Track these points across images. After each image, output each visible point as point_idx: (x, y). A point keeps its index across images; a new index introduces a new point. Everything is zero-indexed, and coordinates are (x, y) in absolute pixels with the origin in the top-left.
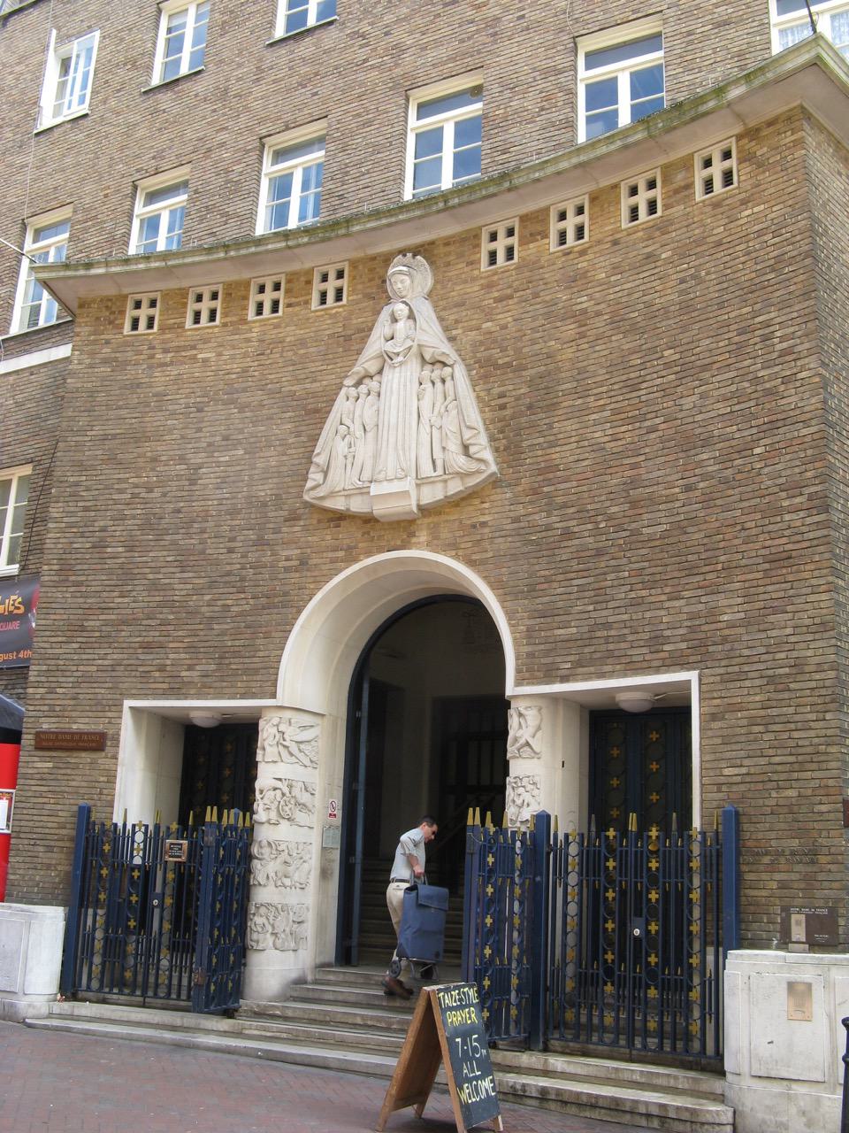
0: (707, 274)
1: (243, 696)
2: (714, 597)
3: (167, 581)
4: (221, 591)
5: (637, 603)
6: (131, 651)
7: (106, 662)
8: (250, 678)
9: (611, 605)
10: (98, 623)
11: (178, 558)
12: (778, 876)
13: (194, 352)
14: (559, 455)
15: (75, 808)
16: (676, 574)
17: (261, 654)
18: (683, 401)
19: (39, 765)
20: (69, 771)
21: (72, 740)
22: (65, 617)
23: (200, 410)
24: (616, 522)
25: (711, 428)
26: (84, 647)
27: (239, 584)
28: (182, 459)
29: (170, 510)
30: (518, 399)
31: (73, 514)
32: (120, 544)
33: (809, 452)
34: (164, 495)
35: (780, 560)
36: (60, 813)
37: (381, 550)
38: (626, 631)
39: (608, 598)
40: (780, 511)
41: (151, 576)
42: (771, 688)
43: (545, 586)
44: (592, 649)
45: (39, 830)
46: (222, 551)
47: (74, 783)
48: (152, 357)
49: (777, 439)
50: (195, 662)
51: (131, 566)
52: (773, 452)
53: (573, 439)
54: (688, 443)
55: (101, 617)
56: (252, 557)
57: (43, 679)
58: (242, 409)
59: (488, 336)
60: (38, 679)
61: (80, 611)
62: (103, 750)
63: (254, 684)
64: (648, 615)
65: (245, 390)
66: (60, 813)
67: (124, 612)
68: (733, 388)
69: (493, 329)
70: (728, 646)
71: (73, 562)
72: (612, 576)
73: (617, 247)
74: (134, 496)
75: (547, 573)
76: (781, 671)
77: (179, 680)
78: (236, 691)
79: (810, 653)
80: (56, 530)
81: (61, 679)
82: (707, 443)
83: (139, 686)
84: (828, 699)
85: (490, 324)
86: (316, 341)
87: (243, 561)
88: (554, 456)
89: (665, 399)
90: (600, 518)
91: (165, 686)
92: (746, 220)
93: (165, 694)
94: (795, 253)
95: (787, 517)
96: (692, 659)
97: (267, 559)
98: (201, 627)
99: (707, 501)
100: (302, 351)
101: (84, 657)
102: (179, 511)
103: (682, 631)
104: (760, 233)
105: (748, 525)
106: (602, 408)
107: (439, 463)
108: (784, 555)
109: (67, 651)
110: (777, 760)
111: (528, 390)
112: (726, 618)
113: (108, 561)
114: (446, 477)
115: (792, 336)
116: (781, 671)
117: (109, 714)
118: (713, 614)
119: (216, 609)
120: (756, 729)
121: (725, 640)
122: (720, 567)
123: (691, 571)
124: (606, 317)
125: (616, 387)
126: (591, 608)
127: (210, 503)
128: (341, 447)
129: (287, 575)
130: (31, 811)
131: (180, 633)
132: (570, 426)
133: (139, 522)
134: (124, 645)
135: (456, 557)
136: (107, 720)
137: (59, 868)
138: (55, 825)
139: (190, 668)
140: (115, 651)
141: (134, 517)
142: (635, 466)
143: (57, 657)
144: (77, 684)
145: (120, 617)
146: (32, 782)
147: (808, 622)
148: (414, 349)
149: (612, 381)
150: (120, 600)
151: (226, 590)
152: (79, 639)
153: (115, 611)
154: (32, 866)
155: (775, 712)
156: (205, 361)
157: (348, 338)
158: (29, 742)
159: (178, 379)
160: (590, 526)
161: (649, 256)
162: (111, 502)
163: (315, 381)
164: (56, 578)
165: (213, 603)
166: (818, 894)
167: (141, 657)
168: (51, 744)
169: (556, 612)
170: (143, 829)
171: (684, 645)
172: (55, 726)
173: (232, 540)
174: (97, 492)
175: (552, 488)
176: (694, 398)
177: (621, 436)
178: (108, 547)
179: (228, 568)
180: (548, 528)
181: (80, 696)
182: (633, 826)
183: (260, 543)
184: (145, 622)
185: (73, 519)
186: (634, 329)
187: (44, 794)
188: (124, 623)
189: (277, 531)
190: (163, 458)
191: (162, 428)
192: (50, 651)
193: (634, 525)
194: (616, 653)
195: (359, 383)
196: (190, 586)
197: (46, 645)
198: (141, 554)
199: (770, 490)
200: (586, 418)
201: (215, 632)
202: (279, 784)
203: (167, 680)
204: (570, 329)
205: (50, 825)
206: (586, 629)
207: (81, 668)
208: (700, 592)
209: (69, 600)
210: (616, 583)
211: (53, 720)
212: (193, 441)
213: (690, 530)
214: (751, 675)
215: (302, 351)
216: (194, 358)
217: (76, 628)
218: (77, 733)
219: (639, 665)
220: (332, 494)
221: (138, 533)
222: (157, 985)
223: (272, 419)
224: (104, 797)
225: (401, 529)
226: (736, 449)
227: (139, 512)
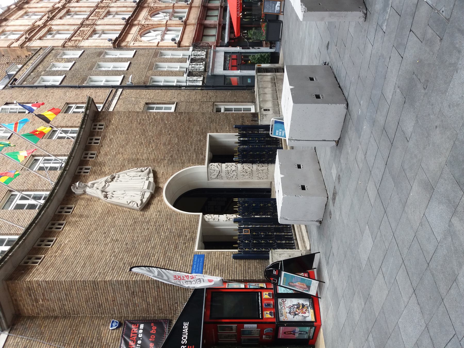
1: (198, 223)
3: (153, 244)
5: (191, 144)
6: (176, 252)
7: (179, 258)
10: (163, 261)
13: (63, 244)
14: (152, 157)
20: (220, 265)
35: (189, 120)
36: (236, 266)
41: (149, 249)
50: (184, 235)
52: (168, 120)
54: (160, 134)
55: (161, 261)
58: (96, 229)
65: (89, 229)
66: (236, 266)
82: (161, 131)
83: (190, 248)
91: (191, 242)
98: (172, 234)
118: (197, 131)
121: (202, 129)
123: (187, 134)
134: (174, 254)
137: (256, 265)
138: (240, 267)
139: (186, 236)
142: (160, 144)
150: (156, 257)
153: (160, 257)
167: (179, 249)
173: (144, 229)
183: (148, 222)
185: (115, 273)
190: (103, 249)
201: (175, 231)
205: (240, 269)
207: (180, 265)
220: (142, 200)
225: (157, 190)
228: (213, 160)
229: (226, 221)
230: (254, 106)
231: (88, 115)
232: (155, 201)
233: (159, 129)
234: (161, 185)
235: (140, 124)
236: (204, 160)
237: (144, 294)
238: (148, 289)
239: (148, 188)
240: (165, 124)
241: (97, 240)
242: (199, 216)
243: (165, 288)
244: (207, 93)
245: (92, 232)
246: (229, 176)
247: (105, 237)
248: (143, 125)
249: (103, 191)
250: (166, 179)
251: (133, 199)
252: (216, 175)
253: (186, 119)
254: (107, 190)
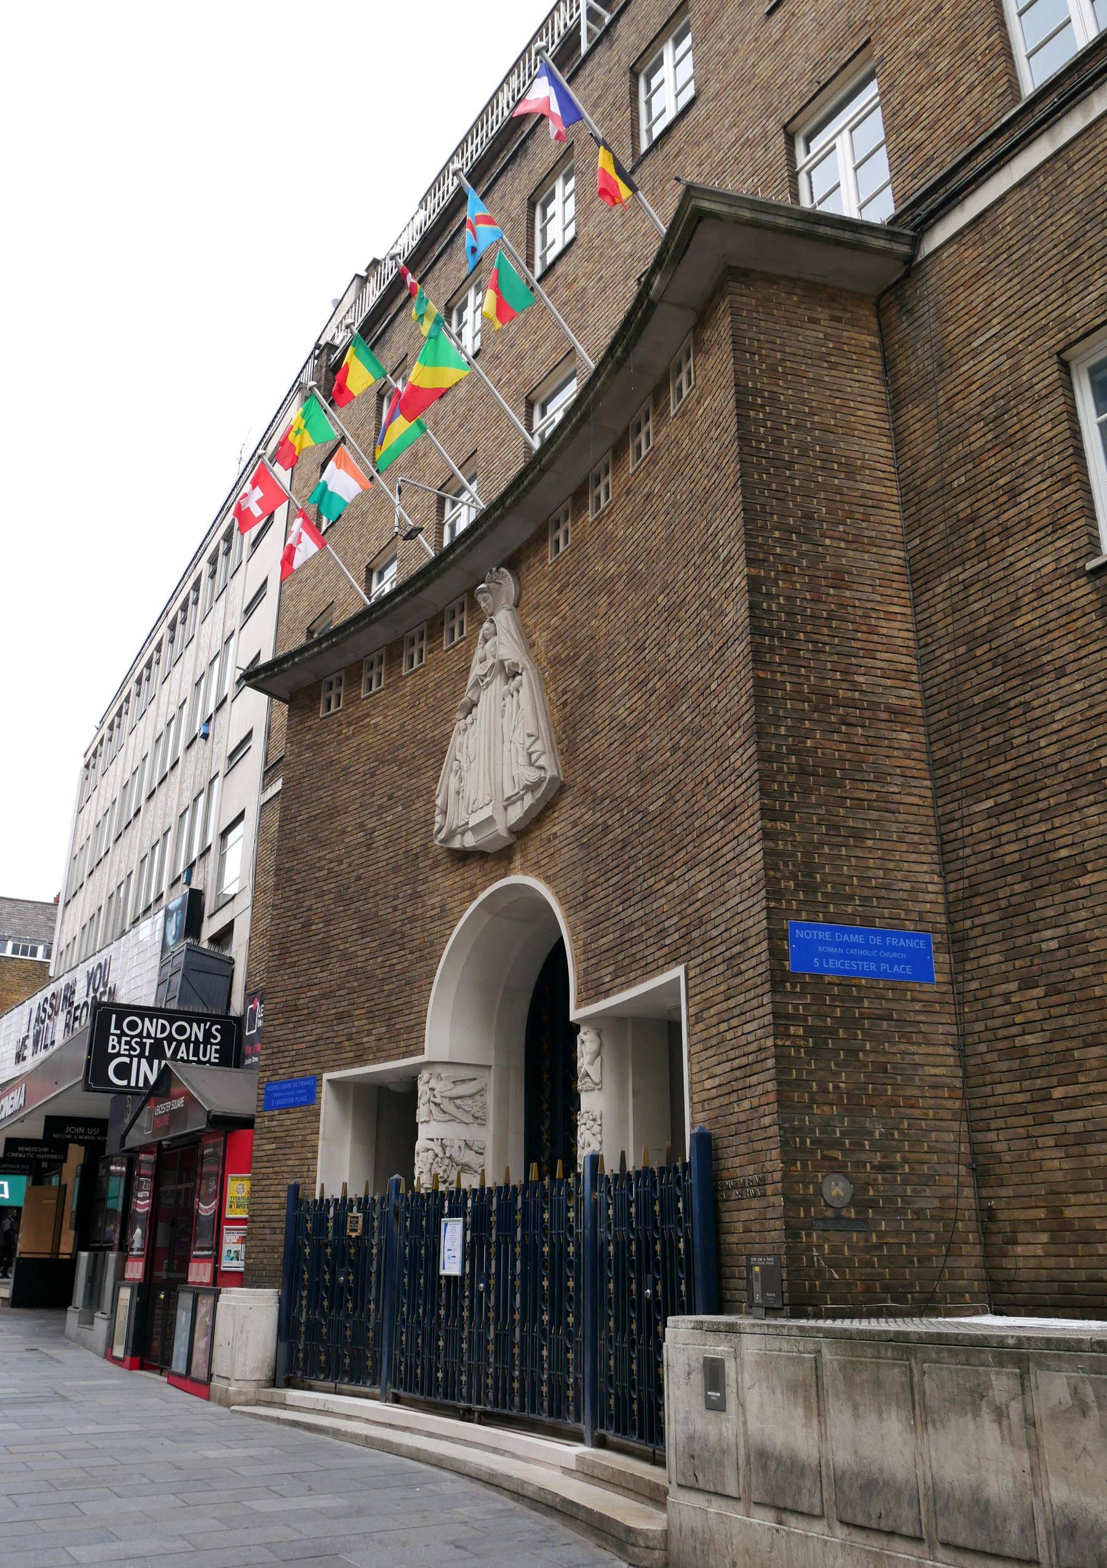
4: (388, 951)
20: (287, 1151)
23: (373, 775)
26: (299, 1024)
47: (290, 1163)
50: (371, 1027)
55: (309, 994)
61: (294, 991)
67: (323, 986)
71: (289, 945)
77: (361, 1047)
83: (335, 1057)
91: (352, 1054)
93: (351, 1064)
98: (375, 990)
128: (453, 782)
138: (277, 1206)
139: (369, 1033)
146: (262, 1165)
148: (497, 666)
152: (294, 1019)
153: (318, 987)
156: (376, 725)
162: (314, 881)
173: (396, 898)
188: (324, 996)
202: (431, 1145)
205: (275, 1206)
227: (333, 885)
234: (518, 861)
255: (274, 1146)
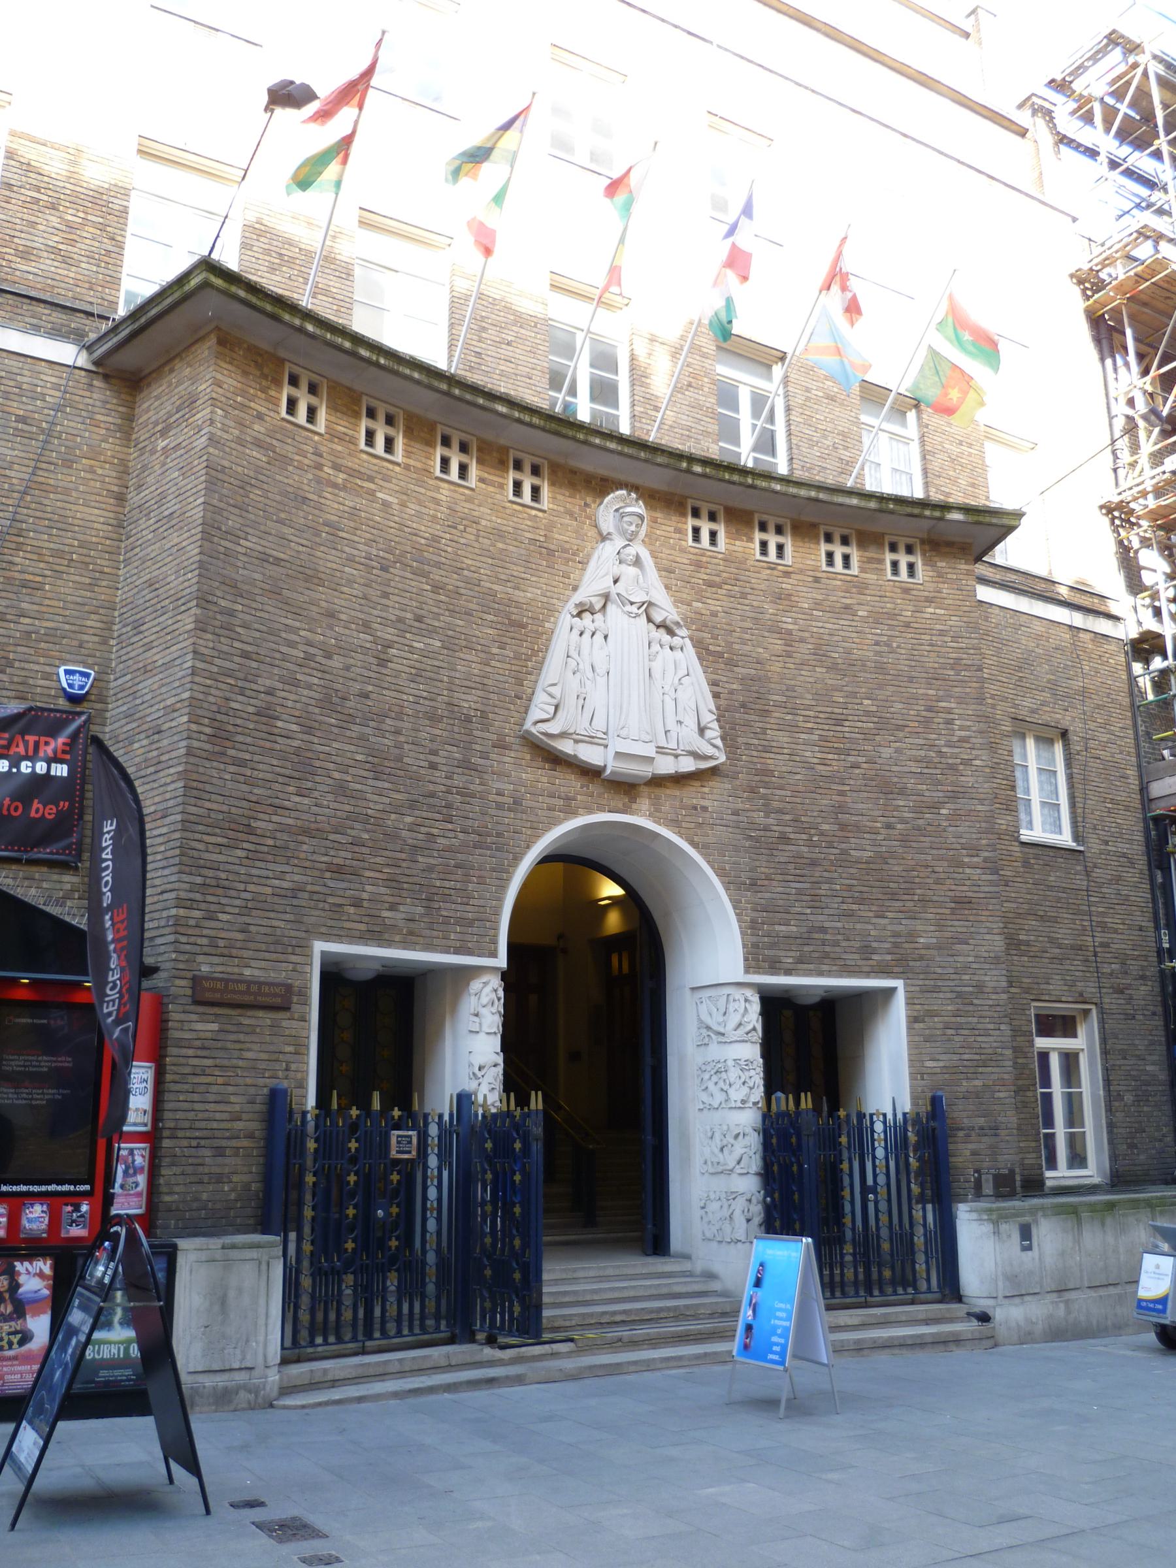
0: (899, 647)
2: (913, 922)
3: (358, 787)
4: (425, 814)
5: (850, 914)
7: (285, 885)
8: (464, 929)
9: (826, 911)
10: (271, 826)
11: (370, 759)
12: (970, 1146)
13: (372, 486)
14: (777, 763)
15: (266, 1091)
16: (880, 896)
17: (475, 902)
18: (881, 749)
19: (199, 1026)
20: (242, 1037)
21: (247, 992)
22: (225, 808)
24: (828, 839)
25: (905, 780)
26: (253, 857)
27: (445, 811)
28: (366, 626)
29: (356, 692)
30: (731, 692)
31: (225, 656)
32: (294, 720)
33: (983, 825)
34: (347, 668)
35: (962, 903)
37: (601, 809)
38: (839, 937)
39: (824, 905)
40: (961, 865)
41: (336, 775)
42: (959, 1001)
43: (766, 882)
44: (811, 948)
45: (203, 1125)
46: (423, 764)
47: (249, 1055)
48: (319, 467)
49: (959, 806)
50: (398, 900)
51: (309, 755)
52: (955, 816)
53: (786, 751)
54: (888, 789)
55: (275, 818)
56: (458, 781)
57: (198, 896)
59: (698, 616)
60: (192, 895)
61: (245, 804)
62: (288, 1009)
63: (468, 937)
64: (858, 926)
65: (438, 565)
66: (233, 1099)
68: (922, 753)
69: (704, 612)
70: (924, 963)
71: (230, 728)
72: (826, 886)
73: (817, 585)
74: (309, 657)
75: (767, 870)
76: (967, 989)
77: (379, 921)
78: (450, 943)
79: (987, 978)
80: (207, 674)
81: (224, 901)
82: (903, 792)
83: (330, 923)
84: (1001, 1014)
85: (700, 605)
86: (516, 540)
87: (449, 782)
88: (769, 761)
89: (866, 742)
90: (813, 831)
91: (363, 927)
92: (928, 616)
94: (970, 662)
95: (968, 871)
96: (896, 969)
97: (476, 787)
98: (403, 856)
99: (904, 840)
100: (500, 545)
101: (254, 872)
102: (366, 696)
103: (887, 945)
104: (942, 633)
105: (937, 869)
106: (810, 731)
107: (673, 735)
108: (966, 900)
109: (230, 859)
110: (966, 1057)
111: (740, 688)
112: (922, 940)
113: (279, 739)
114: (679, 752)
115: (967, 729)
116: (967, 989)
117: (293, 958)
118: (912, 936)
119: (421, 836)
120: (950, 1032)
121: (921, 958)
122: (916, 898)
123: (894, 896)
124: (810, 646)
125: (821, 715)
126: (808, 911)
127: (405, 697)
128: (573, 683)
129: (500, 813)
130: (190, 1097)
131: (378, 860)
132: (783, 738)
133: (316, 696)
134: (307, 864)
135: (680, 835)
136: (291, 967)
137: (235, 1178)
138: (225, 1116)
139: (393, 907)
140: (296, 870)
141: (309, 687)
142: (842, 793)
143: (216, 865)
144: (246, 910)
145: (299, 823)
147: (986, 954)
149: (819, 709)
150: (297, 799)
151: (430, 815)
152: (245, 845)
153: (293, 814)
154: (193, 1179)
155: (962, 1020)
156: (385, 504)
157: (551, 553)
158: (181, 992)
159: (354, 513)
160: (804, 837)
161: (847, 607)
162: (278, 655)
163: (518, 589)
164: (207, 746)
165: (416, 828)
166: (1000, 1158)
167: (331, 883)
168: (218, 995)
169: (777, 909)
170: (881, 1118)
171: (889, 957)
172: (220, 969)
173: (434, 753)
174: (258, 634)
175: (769, 791)
176: (891, 750)
177: (829, 762)
178: (277, 718)
179: (431, 787)
180: (766, 829)
181: (252, 928)
182: (376, 1105)
183: (466, 765)
184: (332, 837)
185: (228, 664)
186: (833, 668)
187: (208, 1071)
188: (306, 832)
189: (485, 756)
190: (343, 617)
191: (338, 574)
192: (206, 856)
193: (843, 846)
194: (832, 955)
195: (579, 615)
196: (387, 801)
197: (201, 846)
198: (323, 741)
199: (954, 846)
200: (797, 735)
201: (420, 866)
203: (366, 919)
204: (778, 645)
205: (218, 1116)
206: (804, 930)
207: (251, 887)
208: (900, 915)
209: (229, 784)
210: (829, 893)
211: (216, 960)
212: (379, 607)
213: (890, 861)
214: (944, 989)
215: (500, 545)
216: (372, 493)
217: (241, 828)
218: (255, 983)
219: (852, 969)
220: (563, 735)
221: (317, 710)
222: (423, 1318)
223: (472, 615)
224: (291, 1074)
225: (625, 789)
226: (928, 805)
227: (316, 681)
228: (775, 1006)
229: (471, 1065)
230: (1097, 1180)
231: (941, 519)
232: (571, 783)
233: (911, 783)
234: (644, 804)
235: (929, 709)
236: (774, 967)
237: (152, 769)
238: (163, 781)
239: (618, 755)
240: (935, 807)
241: (386, 595)
242: (494, 954)
243: (161, 840)
244: (1143, 977)
245: (426, 575)
246: (706, 1076)
247: (400, 620)
248: (927, 722)
249: (606, 597)
250: (674, 824)
251: (570, 704)
252: (709, 1022)
253: (964, 890)
254: (611, 608)
255: (215, 1027)
